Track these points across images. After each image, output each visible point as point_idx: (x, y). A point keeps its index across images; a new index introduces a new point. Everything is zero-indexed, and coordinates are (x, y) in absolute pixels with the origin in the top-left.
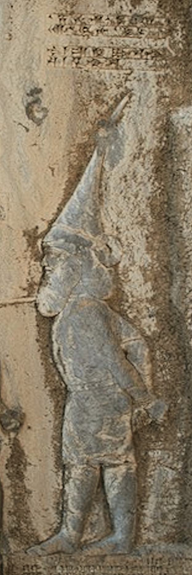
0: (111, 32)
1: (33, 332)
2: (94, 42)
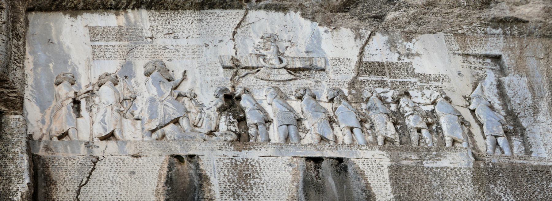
0: (478, 64)
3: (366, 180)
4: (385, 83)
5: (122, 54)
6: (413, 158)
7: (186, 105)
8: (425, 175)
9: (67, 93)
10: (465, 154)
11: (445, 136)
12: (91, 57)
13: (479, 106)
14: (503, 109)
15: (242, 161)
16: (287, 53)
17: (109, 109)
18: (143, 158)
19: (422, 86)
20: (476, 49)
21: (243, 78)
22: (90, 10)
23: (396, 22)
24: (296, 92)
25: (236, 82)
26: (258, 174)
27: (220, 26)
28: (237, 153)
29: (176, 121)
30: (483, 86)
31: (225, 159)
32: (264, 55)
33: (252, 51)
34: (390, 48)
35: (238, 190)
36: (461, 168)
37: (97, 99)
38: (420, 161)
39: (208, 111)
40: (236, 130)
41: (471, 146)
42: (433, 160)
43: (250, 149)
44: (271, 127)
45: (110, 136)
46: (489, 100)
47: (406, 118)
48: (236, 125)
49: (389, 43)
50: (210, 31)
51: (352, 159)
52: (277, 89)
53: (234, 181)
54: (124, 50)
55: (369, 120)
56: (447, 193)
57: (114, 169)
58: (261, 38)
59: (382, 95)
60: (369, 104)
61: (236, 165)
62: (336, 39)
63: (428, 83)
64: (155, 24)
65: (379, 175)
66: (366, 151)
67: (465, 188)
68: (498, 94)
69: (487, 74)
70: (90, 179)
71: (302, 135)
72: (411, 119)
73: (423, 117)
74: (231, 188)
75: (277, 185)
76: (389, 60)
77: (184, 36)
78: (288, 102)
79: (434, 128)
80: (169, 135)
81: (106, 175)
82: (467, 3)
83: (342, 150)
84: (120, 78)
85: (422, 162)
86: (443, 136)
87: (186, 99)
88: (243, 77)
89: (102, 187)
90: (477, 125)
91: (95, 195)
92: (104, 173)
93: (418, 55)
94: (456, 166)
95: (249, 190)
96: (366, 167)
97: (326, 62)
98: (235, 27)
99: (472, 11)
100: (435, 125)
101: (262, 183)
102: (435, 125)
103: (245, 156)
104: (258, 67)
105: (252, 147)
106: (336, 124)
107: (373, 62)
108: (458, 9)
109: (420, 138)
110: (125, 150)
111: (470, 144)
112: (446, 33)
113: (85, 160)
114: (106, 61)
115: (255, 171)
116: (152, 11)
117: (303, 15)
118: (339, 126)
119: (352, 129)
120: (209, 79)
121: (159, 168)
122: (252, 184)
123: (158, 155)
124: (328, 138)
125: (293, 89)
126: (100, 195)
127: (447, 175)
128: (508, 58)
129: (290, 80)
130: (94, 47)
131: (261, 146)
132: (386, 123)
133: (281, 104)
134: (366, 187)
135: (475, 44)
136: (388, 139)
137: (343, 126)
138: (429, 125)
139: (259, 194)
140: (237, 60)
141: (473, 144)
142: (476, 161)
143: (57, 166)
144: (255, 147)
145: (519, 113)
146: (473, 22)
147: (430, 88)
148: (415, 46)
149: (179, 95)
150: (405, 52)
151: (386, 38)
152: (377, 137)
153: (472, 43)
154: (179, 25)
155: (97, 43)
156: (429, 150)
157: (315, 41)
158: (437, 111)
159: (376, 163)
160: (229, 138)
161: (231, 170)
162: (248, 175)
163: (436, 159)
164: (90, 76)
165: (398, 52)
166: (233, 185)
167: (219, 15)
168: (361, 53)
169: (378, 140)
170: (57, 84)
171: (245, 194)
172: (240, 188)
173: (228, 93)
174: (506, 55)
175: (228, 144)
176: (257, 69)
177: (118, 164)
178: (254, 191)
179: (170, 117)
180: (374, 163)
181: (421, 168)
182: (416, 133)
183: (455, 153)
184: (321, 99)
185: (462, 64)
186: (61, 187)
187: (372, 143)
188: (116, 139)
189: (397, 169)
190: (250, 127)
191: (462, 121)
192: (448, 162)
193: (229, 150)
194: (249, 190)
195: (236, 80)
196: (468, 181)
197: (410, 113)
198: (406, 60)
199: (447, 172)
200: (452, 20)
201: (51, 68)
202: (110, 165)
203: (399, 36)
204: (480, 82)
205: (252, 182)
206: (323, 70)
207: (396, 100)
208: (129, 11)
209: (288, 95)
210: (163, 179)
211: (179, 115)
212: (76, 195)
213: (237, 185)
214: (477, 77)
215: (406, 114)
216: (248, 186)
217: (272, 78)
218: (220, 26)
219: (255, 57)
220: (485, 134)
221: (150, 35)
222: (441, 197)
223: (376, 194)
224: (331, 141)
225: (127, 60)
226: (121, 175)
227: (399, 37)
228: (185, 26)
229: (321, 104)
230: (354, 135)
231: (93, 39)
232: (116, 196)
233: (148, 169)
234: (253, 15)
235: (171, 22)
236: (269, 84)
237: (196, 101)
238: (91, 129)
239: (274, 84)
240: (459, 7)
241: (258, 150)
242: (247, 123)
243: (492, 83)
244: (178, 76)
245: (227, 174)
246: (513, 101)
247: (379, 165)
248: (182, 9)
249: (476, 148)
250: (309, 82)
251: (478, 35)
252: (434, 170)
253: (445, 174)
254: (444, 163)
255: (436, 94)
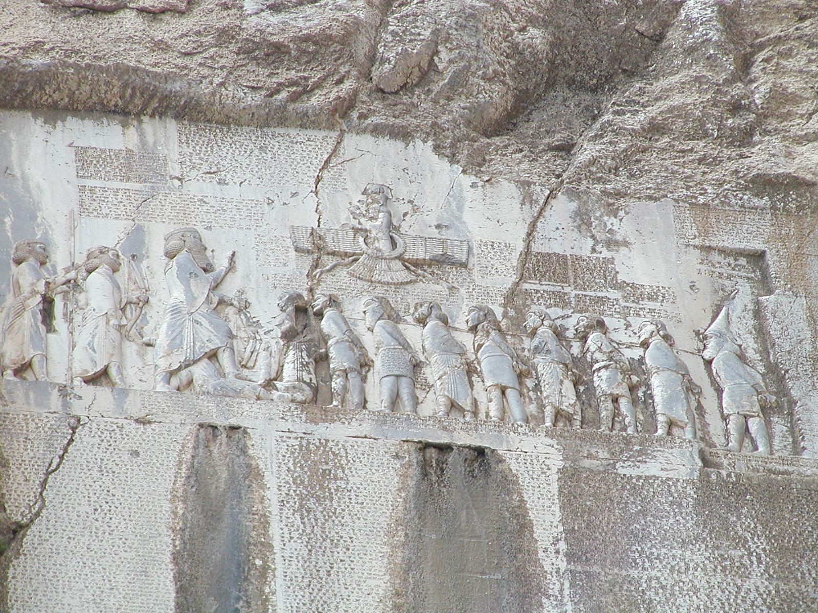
0: (726, 268)
1: (703, 366)
2: (718, 270)
3: (520, 494)
4: (566, 297)
5: (129, 208)
6: (601, 455)
7: (230, 321)
8: (617, 490)
9: (33, 284)
10: (688, 454)
11: (658, 412)
12: (76, 209)
13: (720, 354)
14: (761, 360)
15: (318, 444)
16: (405, 227)
17: (102, 322)
18: (153, 426)
19: (627, 307)
20: (725, 238)
21: (329, 274)
22: (79, 111)
23: (594, 169)
24: (416, 309)
25: (315, 281)
26: (343, 472)
27: (295, 163)
28: (311, 427)
29: (213, 356)
30: (730, 312)
31: (290, 438)
32: (366, 231)
33: (347, 218)
34: (579, 227)
35: (309, 500)
36: (678, 481)
37: (81, 298)
38: (612, 462)
39: (266, 336)
40: (311, 380)
41: (699, 434)
42: (632, 461)
43: (333, 421)
44: (370, 375)
45: (100, 378)
46: (740, 342)
47: (596, 374)
48: (312, 371)
49: (578, 217)
50: (277, 172)
51: (500, 452)
52: (383, 302)
53: (302, 482)
54: (133, 201)
55: (533, 372)
56: (652, 527)
57: (105, 444)
58: (363, 194)
59: (559, 322)
60: (536, 341)
61: (307, 449)
62: (490, 204)
63: (637, 303)
64: (187, 150)
65: (541, 485)
66: (524, 437)
67: (682, 521)
68: (755, 330)
69: (739, 287)
70: (64, 461)
71: (420, 394)
72: (604, 378)
73: (623, 372)
74: (297, 495)
75: (373, 494)
76: (576, 252)
77: (236, 180)
78: (401, 326)
79: (640, 394)
80: (200, 382)
81: (90, 454)
82: (718, 131)
83: (484, 431)
84: (124, 259)
85: (615, 464)
86: (655, 411)
87: (230, 311)
88: (329, 271)
89: (84, 478)
90: (714, 392)
91: (71, 493)
92: (88, 451)
93: (626, 243)
94: (671, 474)
95: (327, 502)
96: (523, 469)
97: (470, 250)
98: (320, 167)
99: (725, 151)
100: (643, 389)
101: (349, 489)
102: (643, 389)
103: (323, 435)
104: (354, 254)
105: (336, 418)
106: (479, 376)
107: (549, 255)
108: (702, 144)
109: (616, 413)
110: (125, 407)
111: (697, 430)
112: (676, 201)
113: (59, 423)
114: (101, 220)
115: (338, 464)
116: (184, 122)
117: (437, 148)
118: (483, 381)
120: (271, 271)
121: (178, 447)
122: (333, 491)
123: (179, 422)
124: (463, 406)
125: (412, 301)
126: (79, 493)
127: (654, 493)
128: (775, 258)
129: (407, 283)
130: (82, 188)
131: (351, 416)
132: (562, 382)
133: (388, 333)
134: (519, 507)
135: (724, 227)
136: (563, 413)
137: (488, 383)
138: (632, 389)
139: (343, 510)
140: (320, 238)
141: (702, 430)
142: (705, 466)
143: (10, 430)
144: (342, 416)
145: (787, 371)
146: (724, 181)
147: (641, 313)
148: (622, 227)
149: (221, 302)
150: (603, 237)
151: (574, 205)
152: (544, 406)
153: (718, 224)
154: (229, 156)
155: (89, 183)
156: (627, 441)
157: (454, 205)
158: (647, 361)
159: (538, 461)
160: (299, 397)
161: (300, 461)
162: (327, 472)
163: (638, 459)
164: (72, 250)
165: (593, 237)
166: (301, 489)
167: (295, 140)
168: (529, 235)
169: (546, 414)
170: (18, 262)
171: (320, 509)
172: (312, 497)
173: (300, 303)
174: (774, 251)
175: (297, 408)
176: (354, 258)
177: (112, 434)
178: (335, 504)
179: (202, 347)
180: (535, 462)
181: (613, 475)
182: (610, 405)
183: (671, 451)
184: (457, 326)
185: (699, 266)
186: (16, 473)
187: (535, 418)
188: (113, 385)
189: (573, 475)
190: (335, 376)
191: (688, 385)
192: (659, 466)
193: (298, 420)
194: (327, 502)
195: (317, 276)
196: (688, 507)
197: (603, 364)
198: (606, 254)
199: (656, 486)
200: (688, 172)
201: (8, 227)
202: (100, 437)
203: (597, 203)
204: (726, 303)
205: (333, 486)
206: (464, 265)
207: (582, 334)
208: (146, 119)
209: (401, 314)
210: (184, 470)
211: (217, 344)
212: (39, 490)
213: (307, 490)
214: (721, 293)
215: (596, 366)
216: (324, 493)
217: (376, 277)
218: (295, 163)
219: (351, 234)
220: (725, 411)
221: (178, 174)
222: (640, 535)
223: (535, 522)
224: (468, 411)
225: (137, 221)
226: (116, 457)
227: (597, 206)
228: (239, 158)
229: (455, 334)
230: (507, 401)
231: (81, 173)
232: (105, 497)
233: (161, 448)
234: (352, 142)
235: (216, 148)
236: (371, 288)
237: (249, 315)
238: (70, 357)
239: (380, 291)
240: (704, 138)
241: (347, 423)
242: (332, 366)
243: (746, 306)
244: (221, 264)
245: (292, 468)
246: (778, 345)
247: (543, 466)
248: (235, 124)
249: (707, 438)
250: (438, 288)
251: (731, 209)
252: (634, 481)
253: (651, 490)
254: (652, 468)
255: (651, 328)
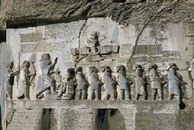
93: (166, 39)
117: (113, 19)
119: (124, 90)
198: (159, 43)
244: (53, 62)
